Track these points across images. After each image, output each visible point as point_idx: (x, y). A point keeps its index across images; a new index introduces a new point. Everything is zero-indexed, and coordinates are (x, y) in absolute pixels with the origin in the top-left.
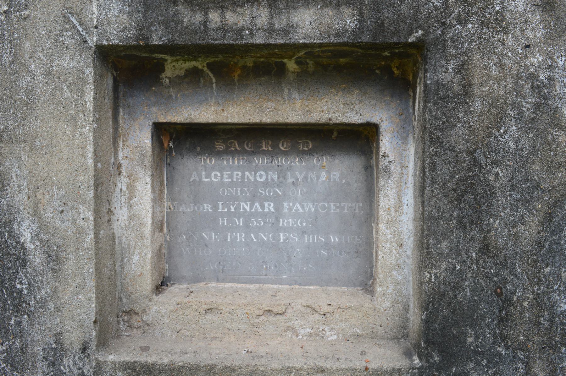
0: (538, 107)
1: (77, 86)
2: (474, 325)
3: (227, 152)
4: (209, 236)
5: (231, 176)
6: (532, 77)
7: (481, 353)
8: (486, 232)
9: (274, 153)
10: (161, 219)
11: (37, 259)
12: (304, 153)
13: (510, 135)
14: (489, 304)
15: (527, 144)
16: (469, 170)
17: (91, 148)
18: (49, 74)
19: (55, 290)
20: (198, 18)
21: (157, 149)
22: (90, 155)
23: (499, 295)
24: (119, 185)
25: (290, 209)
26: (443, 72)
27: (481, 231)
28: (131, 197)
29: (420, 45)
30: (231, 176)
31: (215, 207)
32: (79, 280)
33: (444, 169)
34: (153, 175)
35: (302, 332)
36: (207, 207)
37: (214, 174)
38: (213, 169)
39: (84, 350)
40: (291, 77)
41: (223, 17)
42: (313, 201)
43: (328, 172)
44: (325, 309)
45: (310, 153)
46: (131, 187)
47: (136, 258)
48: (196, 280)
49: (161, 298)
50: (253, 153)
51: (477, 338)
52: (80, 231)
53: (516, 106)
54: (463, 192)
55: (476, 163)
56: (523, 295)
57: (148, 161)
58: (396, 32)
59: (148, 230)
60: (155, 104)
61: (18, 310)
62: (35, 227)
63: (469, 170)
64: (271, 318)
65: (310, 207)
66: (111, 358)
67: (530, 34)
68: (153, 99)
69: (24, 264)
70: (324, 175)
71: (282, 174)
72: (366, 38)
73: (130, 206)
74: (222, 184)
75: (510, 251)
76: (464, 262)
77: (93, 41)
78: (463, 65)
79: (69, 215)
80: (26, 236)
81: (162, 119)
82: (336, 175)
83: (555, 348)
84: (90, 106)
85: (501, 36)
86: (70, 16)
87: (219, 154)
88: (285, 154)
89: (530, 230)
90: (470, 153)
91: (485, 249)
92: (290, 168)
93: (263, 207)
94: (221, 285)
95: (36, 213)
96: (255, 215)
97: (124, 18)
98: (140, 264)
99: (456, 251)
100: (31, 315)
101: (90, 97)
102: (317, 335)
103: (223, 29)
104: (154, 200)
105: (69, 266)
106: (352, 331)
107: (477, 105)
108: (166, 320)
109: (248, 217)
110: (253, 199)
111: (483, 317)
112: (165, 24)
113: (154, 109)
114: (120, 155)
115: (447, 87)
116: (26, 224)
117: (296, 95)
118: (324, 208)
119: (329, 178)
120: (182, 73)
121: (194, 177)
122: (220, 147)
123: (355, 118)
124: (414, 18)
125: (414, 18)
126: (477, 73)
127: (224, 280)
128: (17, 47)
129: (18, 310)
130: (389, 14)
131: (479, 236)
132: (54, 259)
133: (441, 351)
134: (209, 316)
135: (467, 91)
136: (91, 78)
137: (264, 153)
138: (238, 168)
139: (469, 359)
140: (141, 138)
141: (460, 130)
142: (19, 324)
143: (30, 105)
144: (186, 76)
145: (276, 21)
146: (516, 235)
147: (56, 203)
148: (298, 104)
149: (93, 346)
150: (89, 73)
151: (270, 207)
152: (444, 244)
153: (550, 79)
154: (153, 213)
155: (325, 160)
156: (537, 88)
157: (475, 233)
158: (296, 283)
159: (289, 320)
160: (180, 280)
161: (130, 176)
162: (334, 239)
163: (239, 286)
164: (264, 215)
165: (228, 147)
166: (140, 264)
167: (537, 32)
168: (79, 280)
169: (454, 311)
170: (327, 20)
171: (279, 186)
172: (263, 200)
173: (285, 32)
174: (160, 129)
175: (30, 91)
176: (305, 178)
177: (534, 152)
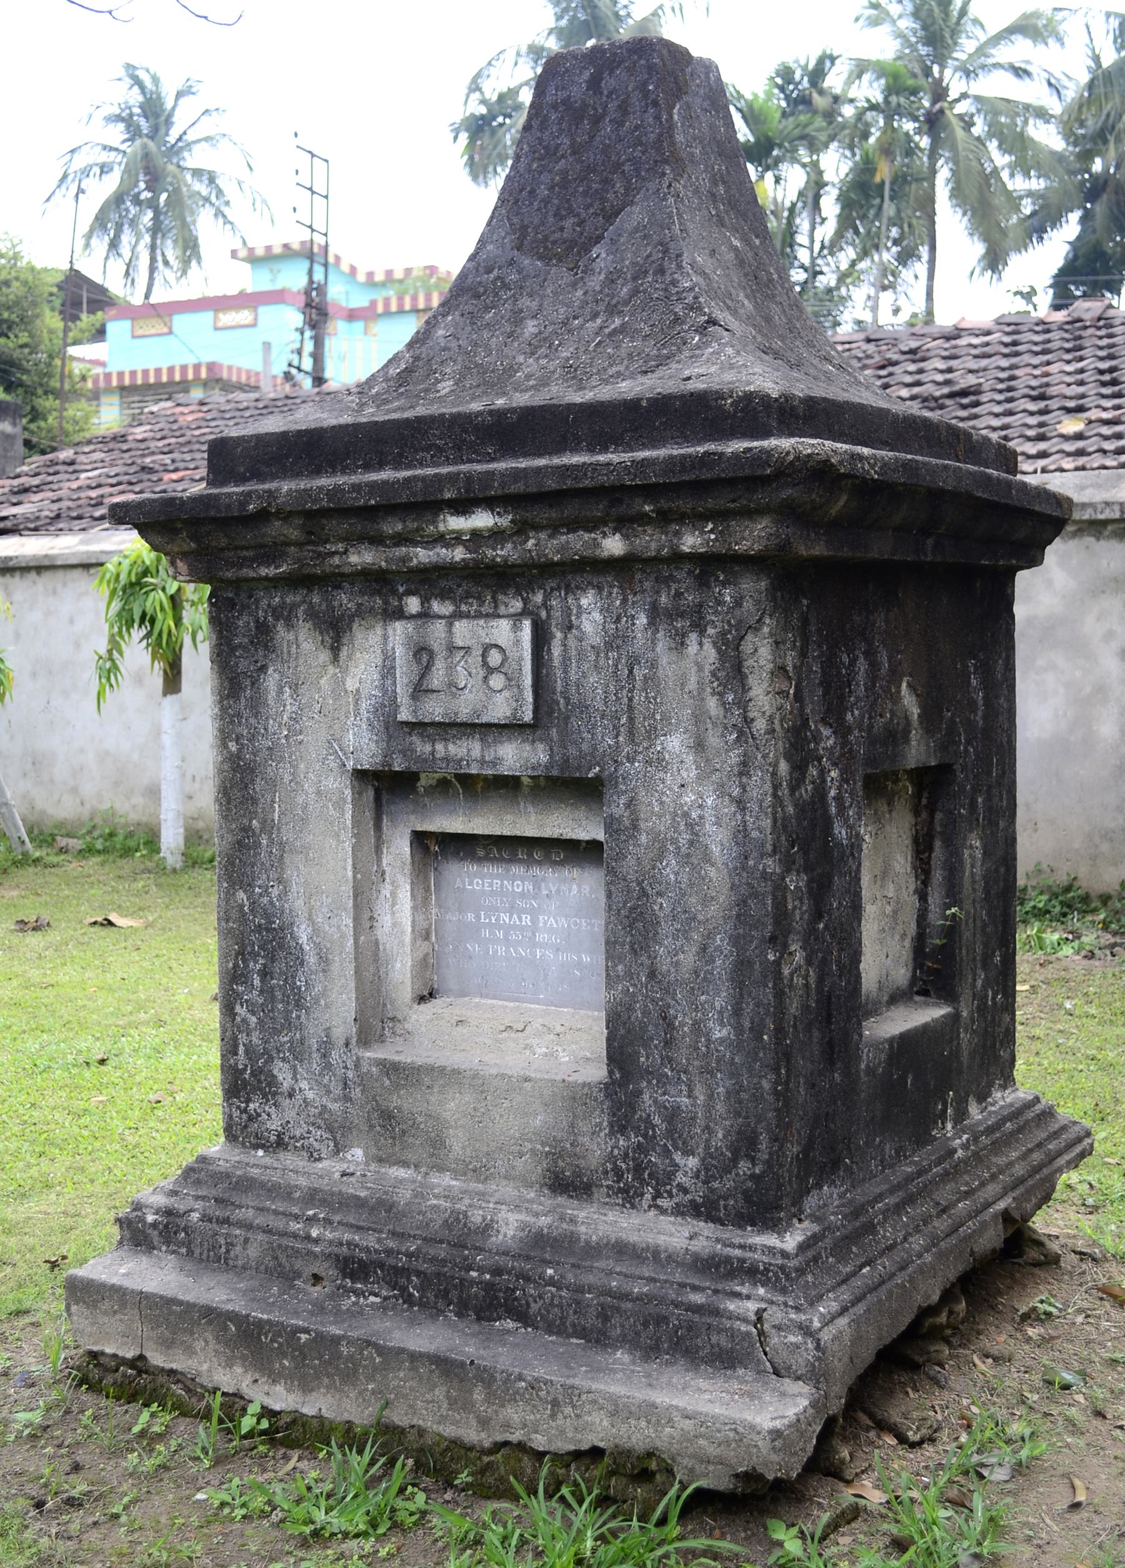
0: (691, 843)
1: (339, 805)
2: (646, 1046)
3: (487, 859)
4: (473, 947)
5: (491, 885)
6: (686, 815)
7: (651, 1073)
8: (653, 958)
9: (529, 862)
10: (425, 925)
11: (311, 959)
12: (556, 863)
13: (670, 868)
14: (656, 1026)
15: (684, 878)
16: (638, 899)
17: (350, 861)
18: (319, 793)
19: (325, 989)
20: (428, 748)
21: (418, 857)
22: (350, 868)
23: (664, 1019)
24: (384, 892)
25: (545, 923)
26: (617, 807)
27: (649, 957)
28: (393, 905)
29: (598, 778)
30: (491, 885)
31: (478, 917)
32: (343, 981)
33: (618, 898)
34: (412, 883)
35: (538, 1051)
36: (470, 917)
37: (476, 881)
38: (475, 876)
39: (347, 1045)
40: (526, 790)
41: (446, 748)
42: (566, 916)
43: (579, 886)
44: (559, 1029)
45: (561, 863)
46: (394, 894)
47: (398, 965)
48: (462, 994)
49: (423, 1007)
50: (510, 861)
51: (647, 1058)
52: (343, 936)
53: (674, 841)
54: (635, 919)
55: (644, 893)
56: (684, 1020)
57: (408, 869)
58: (579, 768)
59: (408, 938)
60: (413, 812)
61: (298, 1005)
62: (310, 930)
63: (638, 899)
64: (513, 1035)
65: (563, 922)
66: (368, 1054)
67: (685, 774)
68: (411, 807)
69: (302, 964)
70: (575, 887)
71: (537, 886)
72: (555, 773)
73: (393, 913)
74: (483, 892)
75: (672, 978)
76: (635, 985)
77: (350, 765)
78: (632, 799)
79: (334, 921)
80: (303, 939)
81: (419, 829)
82: (586, 889)
83: (711, 1073)
84: (349, 823)
85: (661, 775)
86: (334, 741)
87: (480, 860)
88: (539, 863)
89: (688, 959)
90: (639, 884)
91: (652, 975)
92: (544, 879)
93: (520, 919)
94: (484, 1001)
95: (310, 918)
96: (514, 927)
97: (373, 746)
98: (401, 972)
99: (629, 975)
100: (307, 1009)
101: (349, 815)
102: (551, 1055)
103: (447, 759)
104: (414, 908)
105: (335, 968)
106: (582, 1054)
107: (643, 839)
108: (423, 1029)
109: (507, 929)
110: (512, 910)
111: (652, 1039)
112: (403, 752)
113: (412, 817)
114: (384, 862)
115: (619, 820)
116: (303, 927)
117: (530, 809)
118: (576, 924)
119: (579, 892)
120: (434, 782)
121: (458, 884)
122: (481, 853)
124: (592, 754)
125: (592, 754)
126: (643, 808)
127: (487, 996)
129: (298, 1005)
130: (572, 751)
131: (647, 962)
132: (324, 960)
133: (621, 1069)
134: (459, 1029)
135: (635, 827)
136: (349, 799)
137: (520, 861)
138: (498, 876)
139: (642, 1077)
140: (400, 847)
141: (630, 861)
142: (298, 1017)
143: (304, 820)
144: (437, 786)
145: (486, 753)
146: (677, 963)
147: (325, 910)
148: (533, 818)
149: (354, 1041)
150: (348, 792)
151: (527, 920)
152: (620, 967)
153: (701, 817)
154: (413, 922)
155: (576, 872)
156: (690, 826)
157: (643, 958)
158: (552, 1004)
159: (527, 1038)
160: (448, 993)
161: (393, 883)
162: (586, 959)
163: (500, 1003)
164: (522, 929)
165: (487, 854)
166: (401, 972)
167: (690, 773)
168: (343, 981)
169: (629, 1032)
170: (525, 754)
171: (534, 898)
172: (521, 912)
173: (494, 764)
174: (420, 839)
175: (305, 808)
176: (558, 891)
177: (691, 885)
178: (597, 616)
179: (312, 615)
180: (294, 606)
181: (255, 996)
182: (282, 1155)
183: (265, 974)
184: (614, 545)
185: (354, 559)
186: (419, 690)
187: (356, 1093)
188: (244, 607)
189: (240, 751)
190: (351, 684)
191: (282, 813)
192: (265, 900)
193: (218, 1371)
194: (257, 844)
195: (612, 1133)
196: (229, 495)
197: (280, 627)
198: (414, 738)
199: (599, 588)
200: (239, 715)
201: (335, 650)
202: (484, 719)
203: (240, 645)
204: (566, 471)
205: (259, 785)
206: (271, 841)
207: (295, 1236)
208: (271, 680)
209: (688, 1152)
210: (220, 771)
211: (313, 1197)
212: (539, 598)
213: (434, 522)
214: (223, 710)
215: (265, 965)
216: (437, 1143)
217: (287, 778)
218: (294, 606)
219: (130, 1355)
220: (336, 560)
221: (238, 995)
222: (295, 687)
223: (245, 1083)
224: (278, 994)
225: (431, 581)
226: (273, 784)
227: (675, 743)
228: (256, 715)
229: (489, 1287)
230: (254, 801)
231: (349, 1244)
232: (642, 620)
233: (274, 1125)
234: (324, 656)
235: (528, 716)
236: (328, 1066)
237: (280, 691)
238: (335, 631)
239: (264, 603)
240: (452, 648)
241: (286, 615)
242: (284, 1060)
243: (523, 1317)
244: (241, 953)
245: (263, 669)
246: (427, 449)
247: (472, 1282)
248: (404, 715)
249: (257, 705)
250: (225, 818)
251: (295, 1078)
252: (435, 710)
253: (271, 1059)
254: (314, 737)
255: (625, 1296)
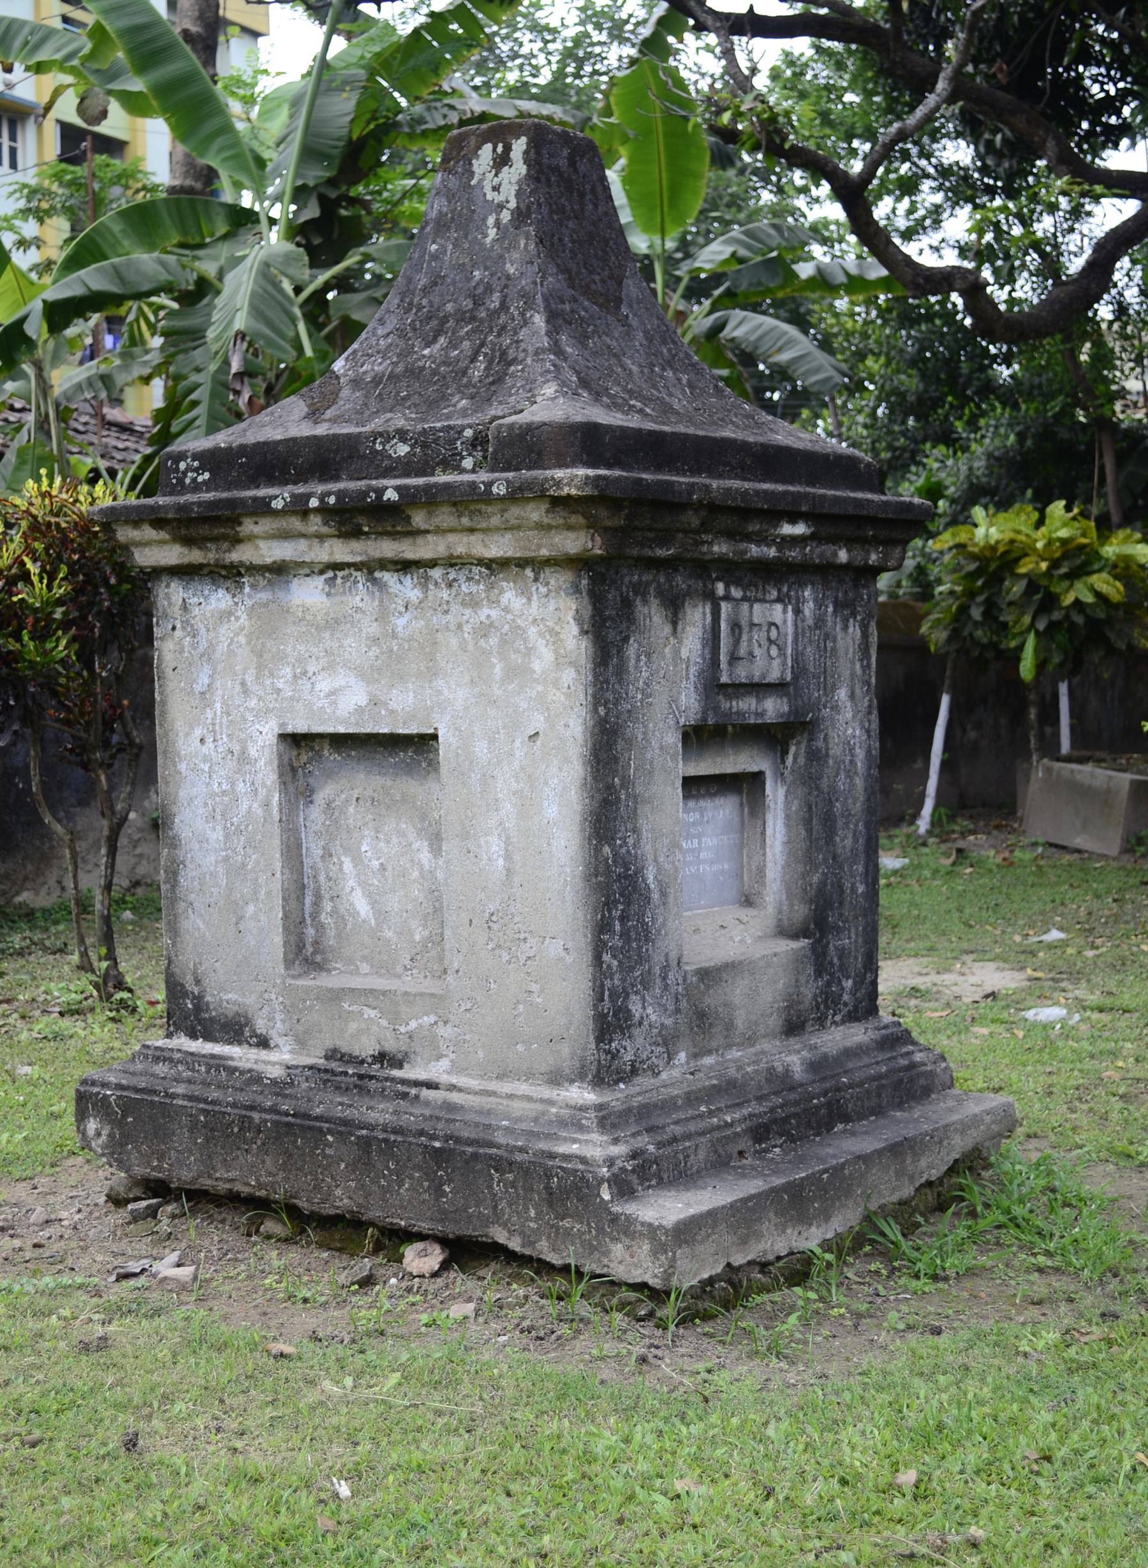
11: (655, 896)
18: (661, 748)
45: (714, 795)
61: (647, 940)
77: (682, 721)
88: (703, 796)
89: (848, 842)
100: (653, 941)
107: (831, 762)
123: (755, 769)
128: (645, 727)
141: (825, 780)
164: (693, 850)
167: (849, 715)
178: (811, 604)
179: (660, 593)
180: (648, 584)
181: (617, 942)
182: (639, 1080)
183: (623, 919)
184: (843, 556)
185: (716, 548)
186: (734, 659)
187: (684, 1004)
188: (613, 582)
189: (607, 714)
190: (684, 653)
191: (636, 769)
192: (624, 850)
193: (777, 1241)
194: (618, 799)
195: (816, 980)
196: (681, 484)
197: (638, 602)
198: (721, 697)
199: (813, 585)
200: (607, 682)
201: (675, 624)
202: (767, 681)
203: (610, 618)
204: (857, 502)
205: (620, 745)
206: (628, 795)
207: (718, 1128)
208: (631, 650)
209: (848, 978)
210: (593, 734)
211: (692, 1098)
212: (785, 589)
213: (776, 527)
214: (596, 675)
215: (623, 911)
216: (729, 1026)
217: (640, 736)
218: (648, 584)
219: (719, 1269)
220: (705, 548)
221: (605, 944)
222: (648, 655)
223: (608, 1023)
224: (633, 935)
225: (732, 570)
226: (630, 743)
227: (842, 694)
228: (620, 681)
229: (829, 1104)
230: (616, 760)
231: (751, 1115)
232: (830, 609)
233: (628, 1057)
234: (668, 629)
235: (789, 677)
236: (666, 987)
237: (638, 660)
238: (674, 607)
239: (627, 579)
240: (752, 625)
241: (641, 590)
242: (636, 993)
243: (846, 1118)
244: (606, 904)
245: (626, 639)
246: (726, 464)
247: (816, 1107)
248: (724, 679)
249: (621, 671)
250: (595, 778)
251: (644, 1008)
252: (742, 674)
253: (627, 996)
254: (660, 702)
255: (879, 1077)
